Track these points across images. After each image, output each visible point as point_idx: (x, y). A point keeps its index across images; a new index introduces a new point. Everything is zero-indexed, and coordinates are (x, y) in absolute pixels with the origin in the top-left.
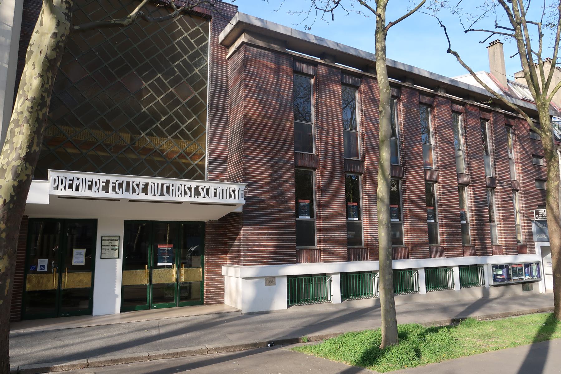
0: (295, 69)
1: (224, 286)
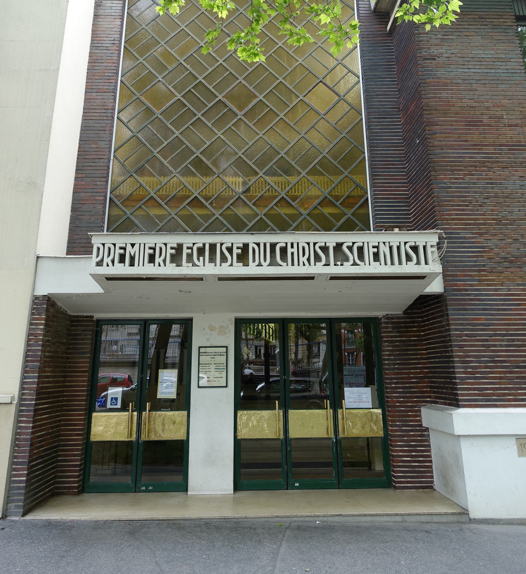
0: (517, 14)
1: (429, 451)
